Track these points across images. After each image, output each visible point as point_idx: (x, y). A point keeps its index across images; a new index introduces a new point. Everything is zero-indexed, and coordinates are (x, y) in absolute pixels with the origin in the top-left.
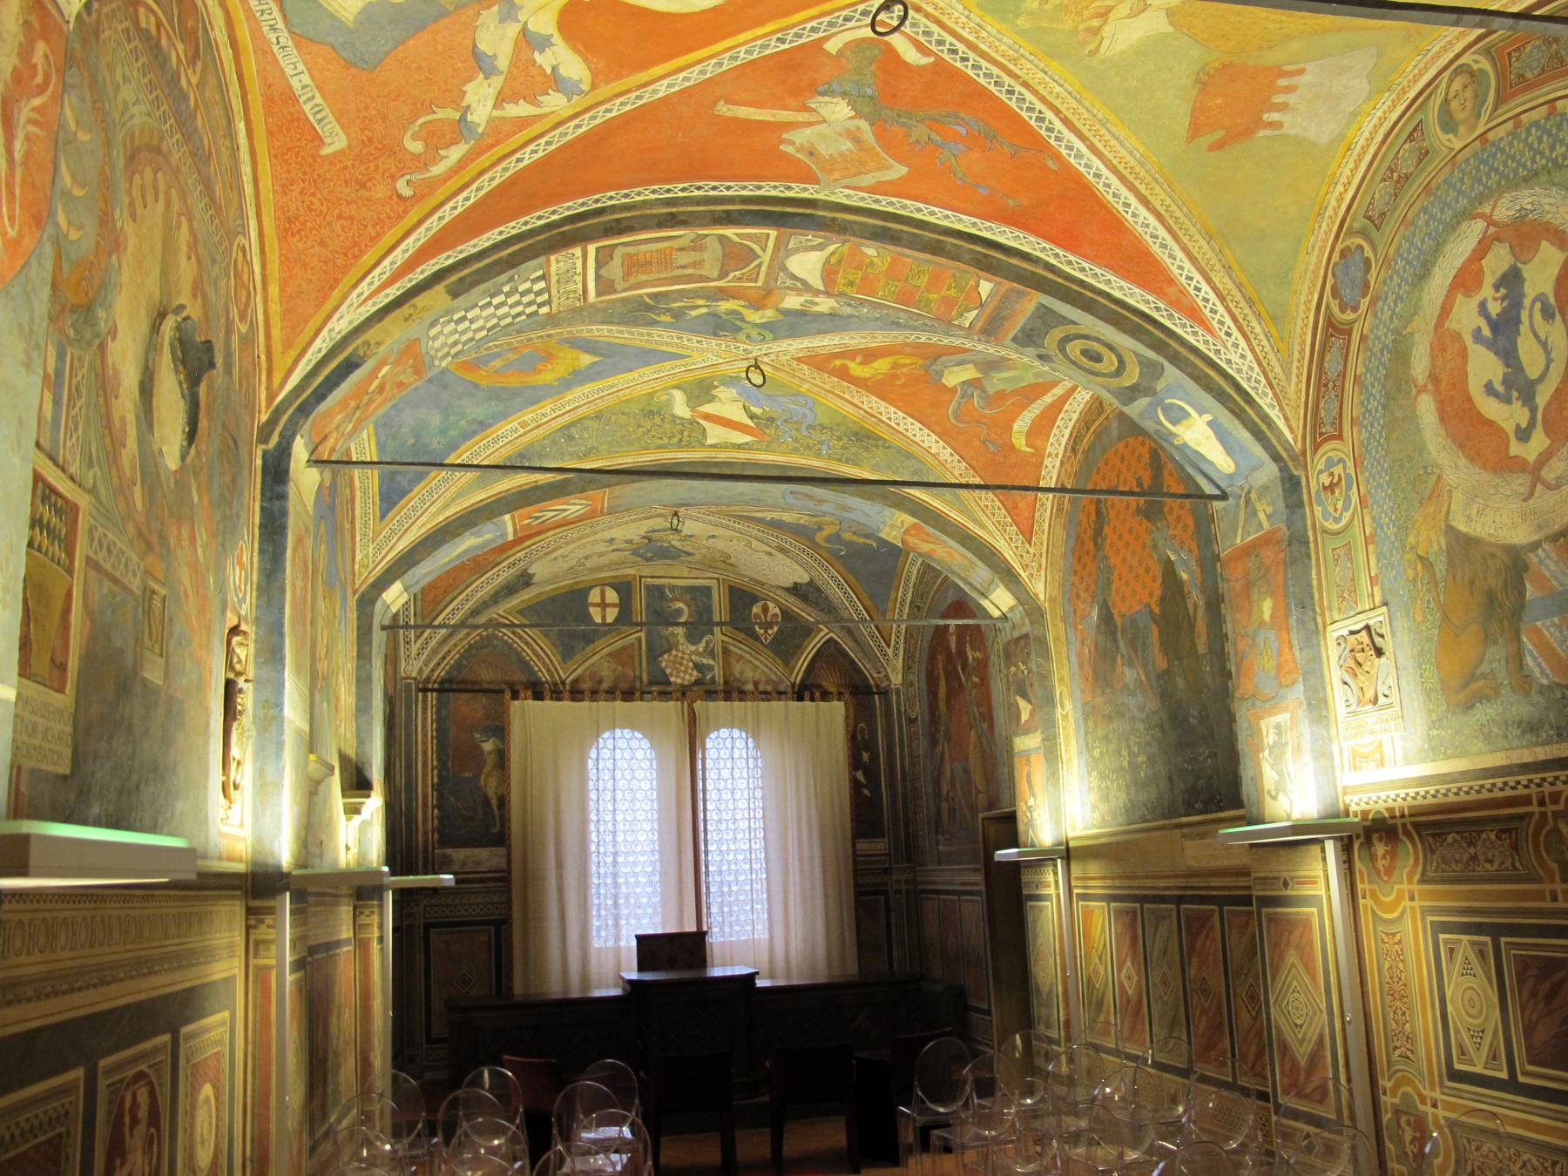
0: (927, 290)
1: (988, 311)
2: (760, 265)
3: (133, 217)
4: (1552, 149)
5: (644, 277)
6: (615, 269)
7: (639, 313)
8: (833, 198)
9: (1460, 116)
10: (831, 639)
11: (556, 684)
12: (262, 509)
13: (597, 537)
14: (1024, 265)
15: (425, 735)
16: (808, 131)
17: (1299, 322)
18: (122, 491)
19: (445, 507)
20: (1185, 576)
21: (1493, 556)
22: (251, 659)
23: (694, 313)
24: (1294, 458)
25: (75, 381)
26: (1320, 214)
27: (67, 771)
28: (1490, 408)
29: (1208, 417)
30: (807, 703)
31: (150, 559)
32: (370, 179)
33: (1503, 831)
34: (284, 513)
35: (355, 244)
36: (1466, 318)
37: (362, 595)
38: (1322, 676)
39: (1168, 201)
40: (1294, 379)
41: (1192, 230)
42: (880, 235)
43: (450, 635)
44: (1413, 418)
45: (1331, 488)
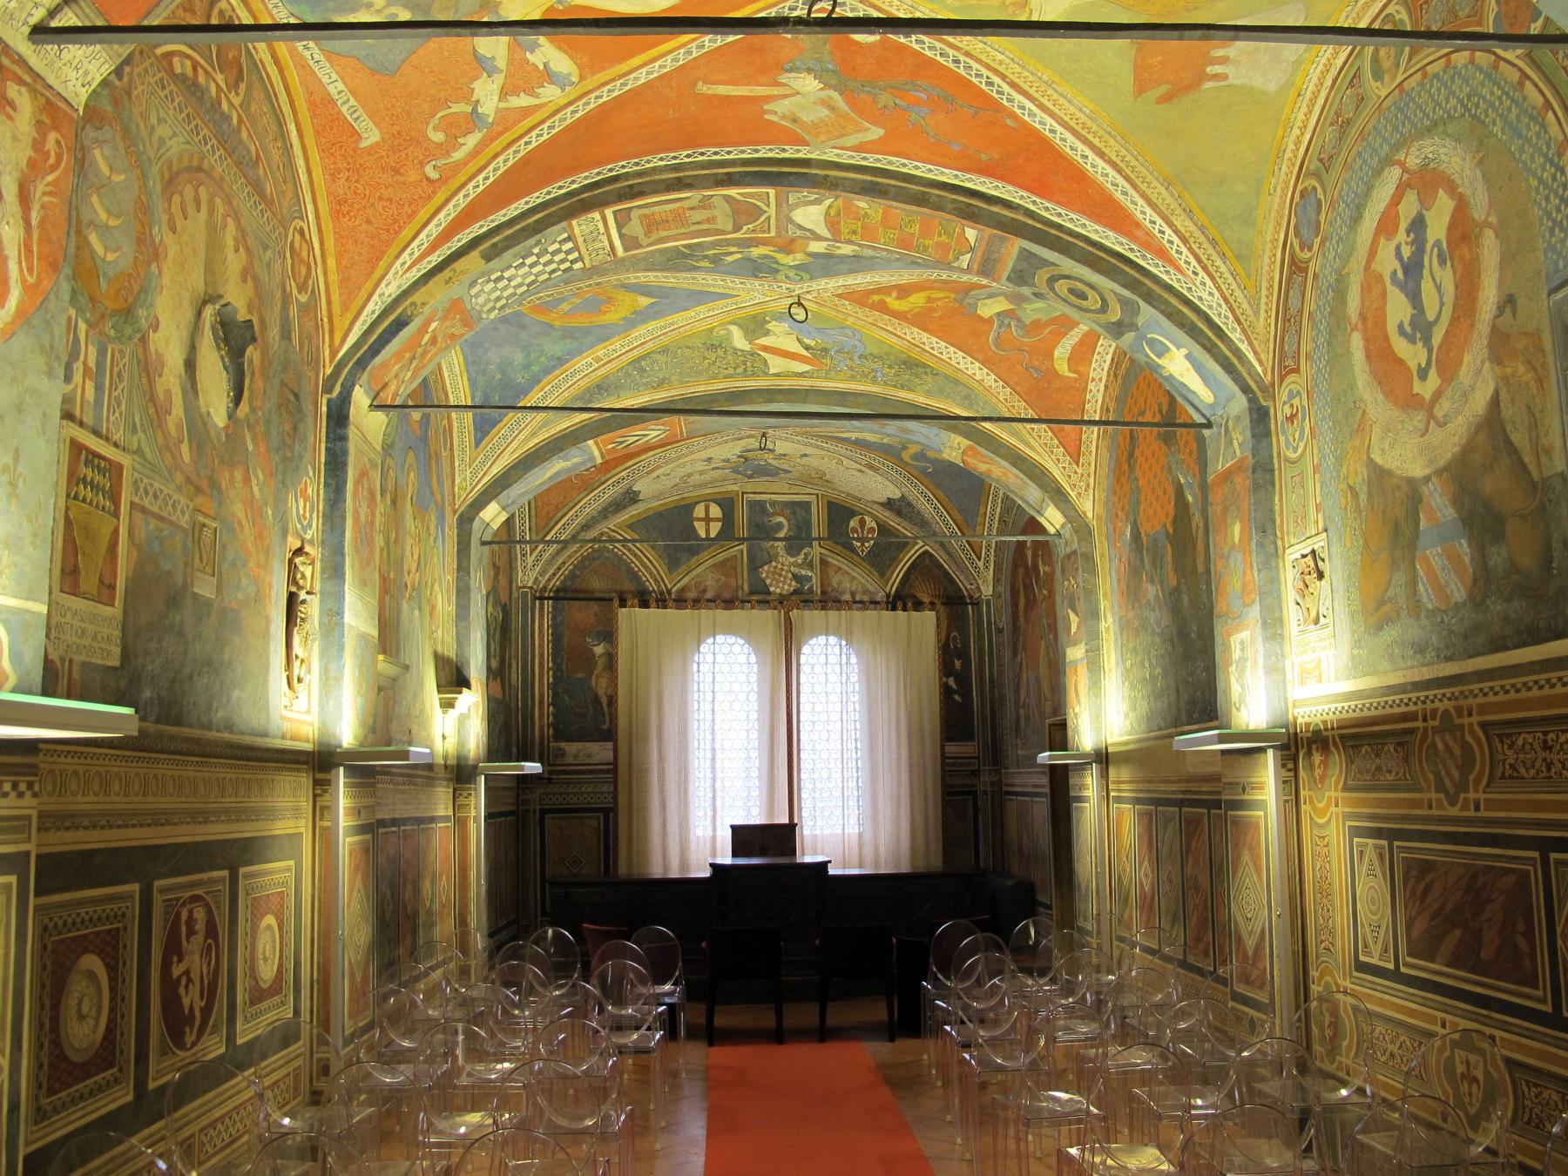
2: (769, 218)
3: (174, 230)
4: (1447, 101)
5: (665, 233)
6: (635, 228)
7: (679, 260)
8: (824, 157)
9: (1386, 64)
10: (926, 552)
11: (662, 593)
12: (327, 449)
14: (1005, 212)
15: (542, 639)
17: (1266, 260)
18: (170, 448)
19: (533, 435)
20: (1190, 499)
21: (1399, 487)
22: (318, 575)
23: (730, 259)
24: (1263, 389)
25: (116, 370)
26: (1279, 156)
27: (117, 664)
28: (1401, 347)
29: (1184, 351)
30: (900, 613)
31: (199, 500)
33: (1399, 744)
34: (345, 452)
35: (395, 221)
36: (1387, 263)
37: (462, 515)
38: (1279, 596)
39: (1123, 152)
40: (1263, 315)
41: (1150, 178)
43: (558, 553)
44: (1347, 354)
45: (1291, 418)
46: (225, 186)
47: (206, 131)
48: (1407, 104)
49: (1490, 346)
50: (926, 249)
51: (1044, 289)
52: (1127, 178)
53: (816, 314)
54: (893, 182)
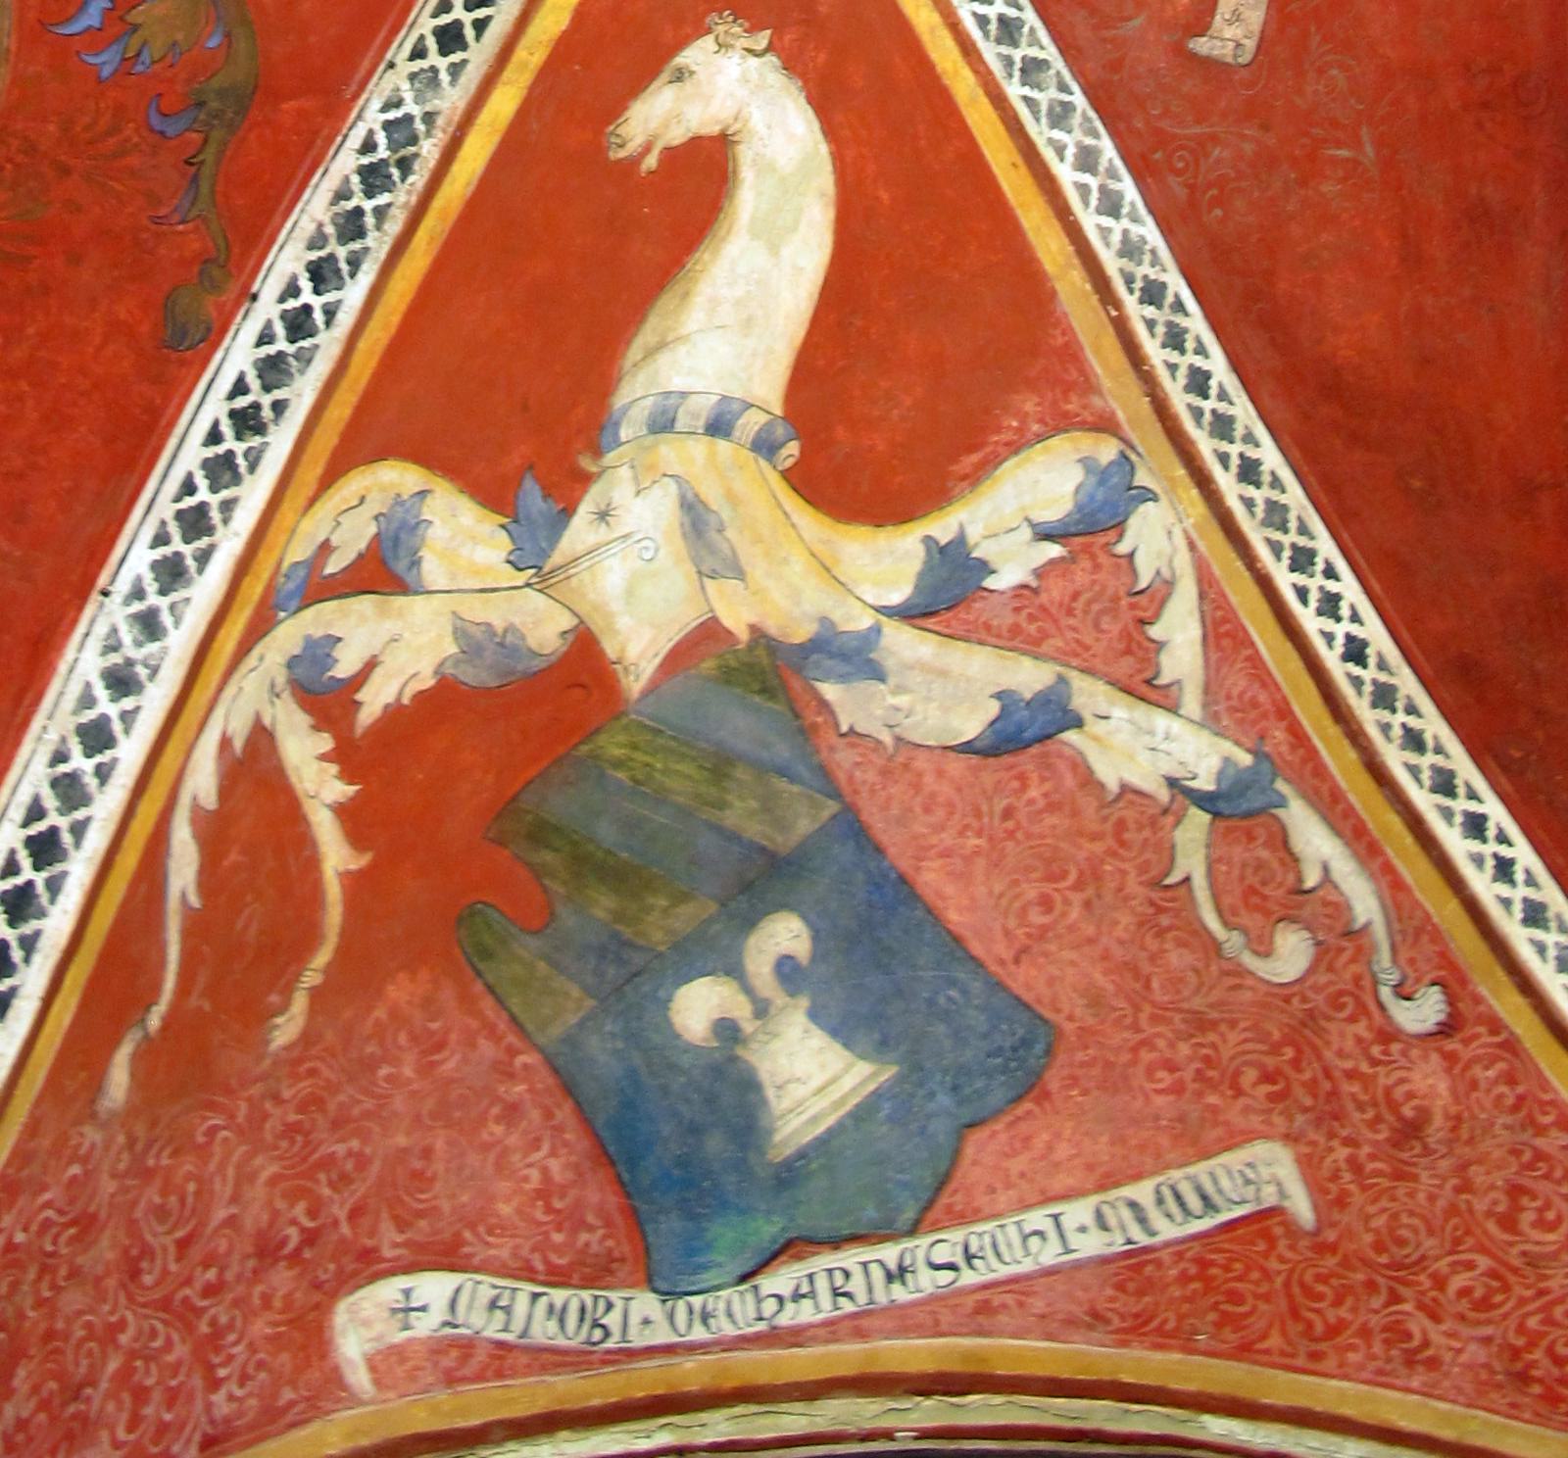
32: (1393, 1106)
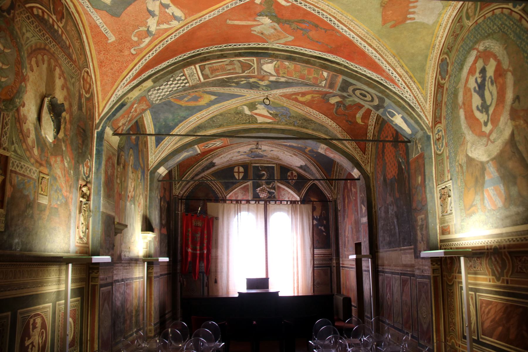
0: (308, 75)
1: (328, 81)
2: (254, 68)
5: (218, 74)
6: (207, 71)
7: (223, 83)
8: (273, 47)
9: (471, 14)
12: (96, 149)
13: (234, 151)
16: (259, 27)
17: (429, 84)
19: (176, 143)
20: (403, 167)
21: (477, 165)
23: (242, 83)
26: (434, 47)
28: (478, 114)
29: (401, 115)
31: (42, 168)
35: (121, 69)
36: (472, 84)
39: (378, 45)
40: (428, 103)
41: (388, 54)
42: (289, 58)
44: (458, 117)
46: (55, 55)
47: (47, 35)
48: (479, 28)
49: (511, 115)
50: (309, 79)
51: (351, 93)
52: (380, 54)
53: (273, 102)
54: (298, 56)
